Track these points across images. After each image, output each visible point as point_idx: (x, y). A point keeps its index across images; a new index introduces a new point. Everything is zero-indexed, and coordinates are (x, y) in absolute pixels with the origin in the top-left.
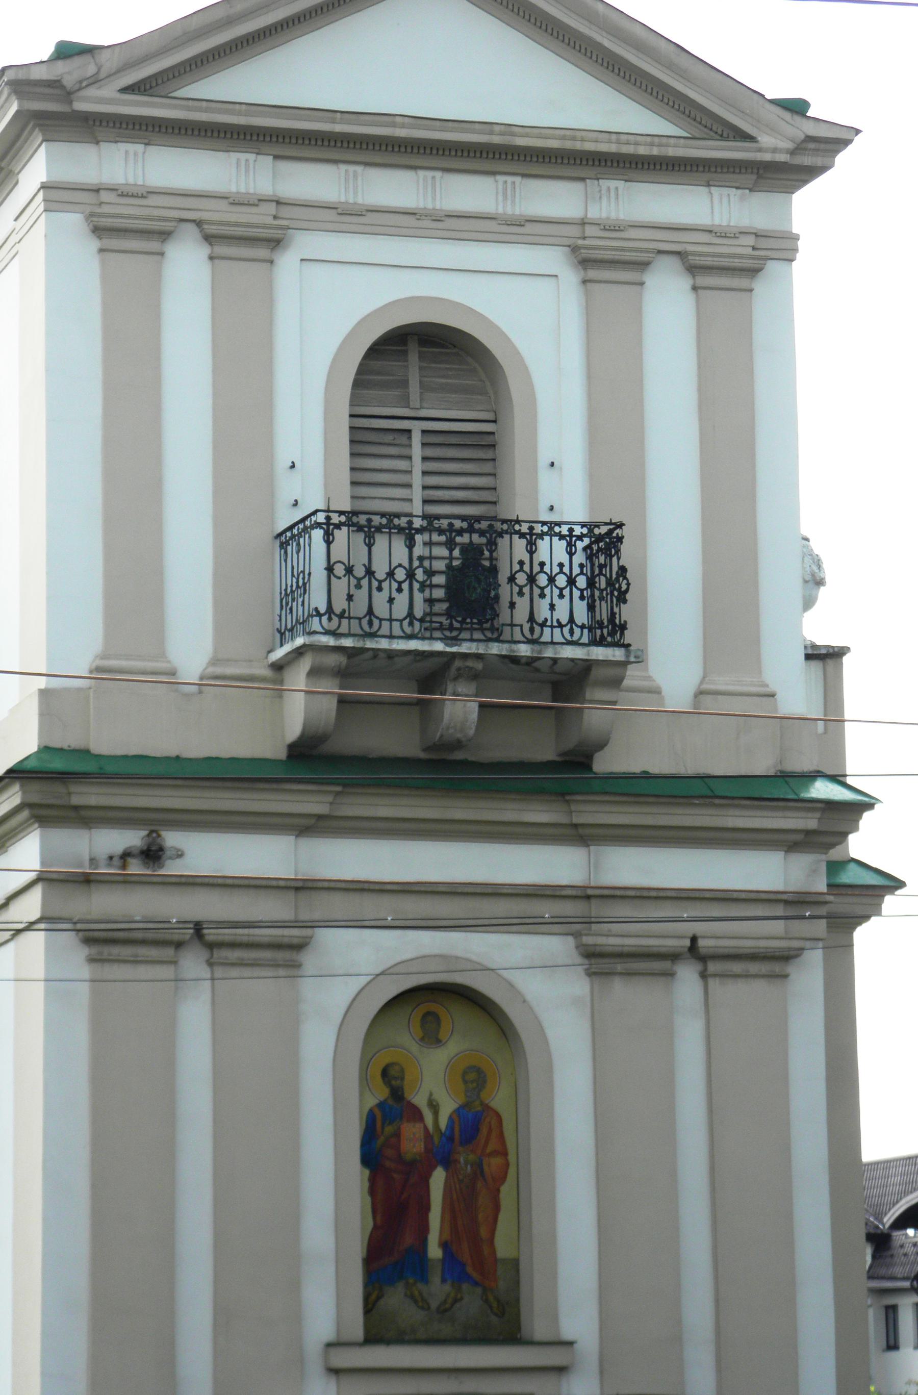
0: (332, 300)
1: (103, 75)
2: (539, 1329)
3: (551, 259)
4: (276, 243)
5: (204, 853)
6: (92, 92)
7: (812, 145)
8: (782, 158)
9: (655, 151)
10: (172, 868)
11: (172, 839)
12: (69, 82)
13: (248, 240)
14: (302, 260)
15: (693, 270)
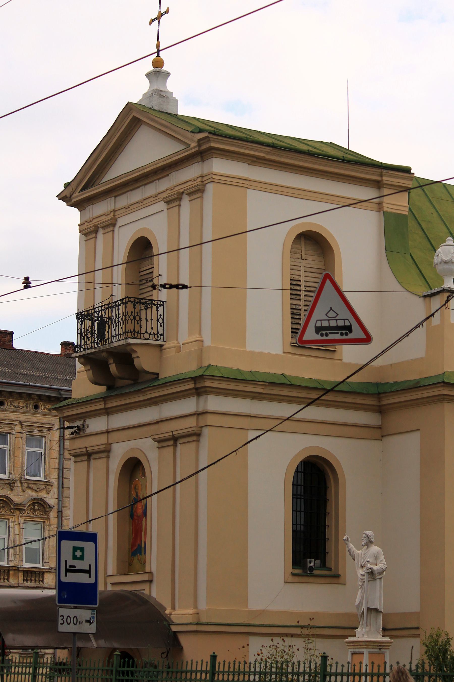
0: (124, 238)
1: (74, 190)
2: (147, 570)
3: (162, 205)
4: (114, 225)
5: (96, 425)
6: (74, 195)
7: (202, 142)
8: (197, 149)
9: (170, 160)
10: (88, 431)
11: (88, 422)
12: (68, 195)
13: (111, 225)
14: (119, 227)
15: (189, 194)
